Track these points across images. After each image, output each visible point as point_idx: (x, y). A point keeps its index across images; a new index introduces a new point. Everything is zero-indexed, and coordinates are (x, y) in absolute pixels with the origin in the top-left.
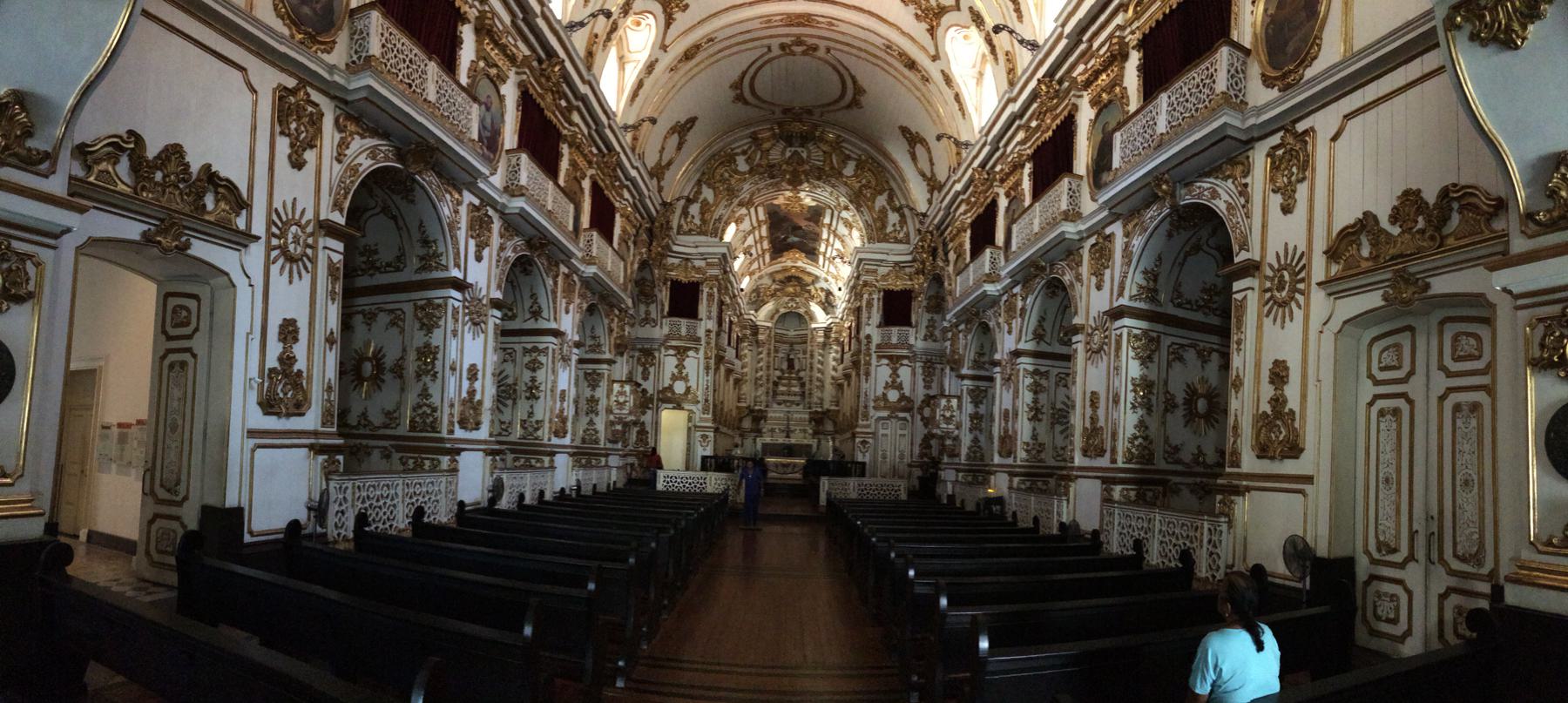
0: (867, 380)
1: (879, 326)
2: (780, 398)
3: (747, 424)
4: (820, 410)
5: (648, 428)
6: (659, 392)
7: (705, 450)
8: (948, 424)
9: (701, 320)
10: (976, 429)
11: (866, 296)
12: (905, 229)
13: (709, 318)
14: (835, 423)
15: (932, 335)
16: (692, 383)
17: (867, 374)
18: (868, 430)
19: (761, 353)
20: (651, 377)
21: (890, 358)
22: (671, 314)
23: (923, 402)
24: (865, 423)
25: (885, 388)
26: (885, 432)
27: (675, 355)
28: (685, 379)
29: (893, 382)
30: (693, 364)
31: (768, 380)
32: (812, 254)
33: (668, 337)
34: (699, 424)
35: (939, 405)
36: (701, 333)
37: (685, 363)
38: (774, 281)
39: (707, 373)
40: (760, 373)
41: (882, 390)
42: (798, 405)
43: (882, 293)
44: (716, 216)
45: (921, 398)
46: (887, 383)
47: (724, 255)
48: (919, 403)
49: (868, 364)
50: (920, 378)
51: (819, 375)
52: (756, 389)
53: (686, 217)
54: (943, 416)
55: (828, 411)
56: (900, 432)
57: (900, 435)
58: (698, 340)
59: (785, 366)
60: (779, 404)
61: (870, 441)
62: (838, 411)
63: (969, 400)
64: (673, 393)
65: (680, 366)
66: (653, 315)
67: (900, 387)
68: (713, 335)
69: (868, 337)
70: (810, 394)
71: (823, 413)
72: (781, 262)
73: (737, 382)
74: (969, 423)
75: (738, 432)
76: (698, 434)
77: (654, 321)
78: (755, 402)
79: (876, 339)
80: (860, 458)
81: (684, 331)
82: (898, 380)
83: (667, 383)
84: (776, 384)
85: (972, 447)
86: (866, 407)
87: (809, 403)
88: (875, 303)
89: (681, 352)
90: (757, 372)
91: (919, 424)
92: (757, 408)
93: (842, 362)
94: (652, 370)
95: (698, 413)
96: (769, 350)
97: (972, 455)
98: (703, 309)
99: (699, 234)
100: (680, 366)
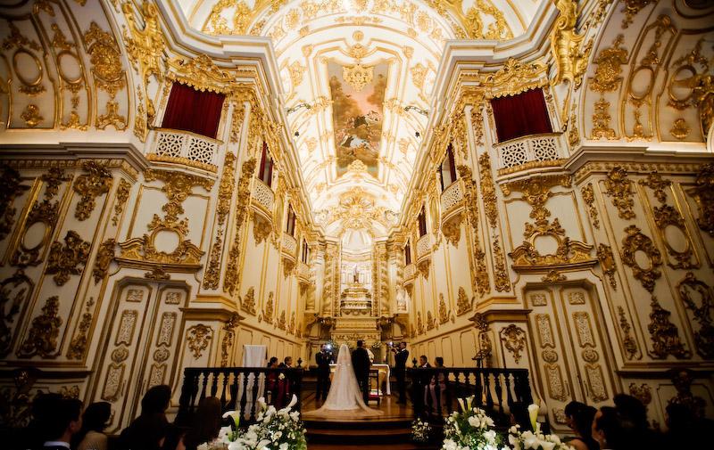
0: (493, 223)
2: (347, 307)
3: (315, 332)
4: (387, 316)
5: (62, 313)
6: (111, 245)
7: (197, 356)
11: (468, 110)
12: (506, 30)
13: (234, 140)
14: (403, 327)
15: (605, 128)
17: (493, 216)
20: (95, 215)
22: (169, 123)
23: (630, 238)
24: (504, 294)
25: (527, 236)
27: (164, 190)
28: (181, 229)
30: (196, 208)
31: (336, 291)
32: (372, 163)
34: (191, 306)
37: (184, 205)
39: (221, 221)
40: (328, 284)
42: (364, 313)
44: (256, 21)
45: (621, 236)
46: (529, 228)
47: (259, 57)
48: (620, 245)
49: (490, 199)
50: (603, 201)
51: (384, 283)
52: (325, 299)
55: (397, 315)
56: (571, 310)
57: (576, 315)
58: (214, 169)
59: (352, 279)
60: (347, 314)
61: (523, 326)
62: (407, 315)
64: (151, 251)
65: (174, 208)
66: (122, 111)
67: (555, 230)
68: (238, 166)
69: (485, 161)
70: (376, 302)
71: (390, 319)
73: (304, 287)
75: (306, 340)
76: (189, 324)
77: (122, 120)
78: (324, 310)
79: (497, 162)
80: (511, 364)
81: (185, 151)
82: (551, 220)
83: (140, 231)
84: (344, 296)
86: (501, 268)
87: (376, 311)
88: (485, 114)
89: (178, 182)
90: (325, 282)
91: (637, 286)
92: (325, 316)
93: (408, 261)
94: (99, 201)
96: (337, 264)
98: (224, 128)
100: (174, 208)
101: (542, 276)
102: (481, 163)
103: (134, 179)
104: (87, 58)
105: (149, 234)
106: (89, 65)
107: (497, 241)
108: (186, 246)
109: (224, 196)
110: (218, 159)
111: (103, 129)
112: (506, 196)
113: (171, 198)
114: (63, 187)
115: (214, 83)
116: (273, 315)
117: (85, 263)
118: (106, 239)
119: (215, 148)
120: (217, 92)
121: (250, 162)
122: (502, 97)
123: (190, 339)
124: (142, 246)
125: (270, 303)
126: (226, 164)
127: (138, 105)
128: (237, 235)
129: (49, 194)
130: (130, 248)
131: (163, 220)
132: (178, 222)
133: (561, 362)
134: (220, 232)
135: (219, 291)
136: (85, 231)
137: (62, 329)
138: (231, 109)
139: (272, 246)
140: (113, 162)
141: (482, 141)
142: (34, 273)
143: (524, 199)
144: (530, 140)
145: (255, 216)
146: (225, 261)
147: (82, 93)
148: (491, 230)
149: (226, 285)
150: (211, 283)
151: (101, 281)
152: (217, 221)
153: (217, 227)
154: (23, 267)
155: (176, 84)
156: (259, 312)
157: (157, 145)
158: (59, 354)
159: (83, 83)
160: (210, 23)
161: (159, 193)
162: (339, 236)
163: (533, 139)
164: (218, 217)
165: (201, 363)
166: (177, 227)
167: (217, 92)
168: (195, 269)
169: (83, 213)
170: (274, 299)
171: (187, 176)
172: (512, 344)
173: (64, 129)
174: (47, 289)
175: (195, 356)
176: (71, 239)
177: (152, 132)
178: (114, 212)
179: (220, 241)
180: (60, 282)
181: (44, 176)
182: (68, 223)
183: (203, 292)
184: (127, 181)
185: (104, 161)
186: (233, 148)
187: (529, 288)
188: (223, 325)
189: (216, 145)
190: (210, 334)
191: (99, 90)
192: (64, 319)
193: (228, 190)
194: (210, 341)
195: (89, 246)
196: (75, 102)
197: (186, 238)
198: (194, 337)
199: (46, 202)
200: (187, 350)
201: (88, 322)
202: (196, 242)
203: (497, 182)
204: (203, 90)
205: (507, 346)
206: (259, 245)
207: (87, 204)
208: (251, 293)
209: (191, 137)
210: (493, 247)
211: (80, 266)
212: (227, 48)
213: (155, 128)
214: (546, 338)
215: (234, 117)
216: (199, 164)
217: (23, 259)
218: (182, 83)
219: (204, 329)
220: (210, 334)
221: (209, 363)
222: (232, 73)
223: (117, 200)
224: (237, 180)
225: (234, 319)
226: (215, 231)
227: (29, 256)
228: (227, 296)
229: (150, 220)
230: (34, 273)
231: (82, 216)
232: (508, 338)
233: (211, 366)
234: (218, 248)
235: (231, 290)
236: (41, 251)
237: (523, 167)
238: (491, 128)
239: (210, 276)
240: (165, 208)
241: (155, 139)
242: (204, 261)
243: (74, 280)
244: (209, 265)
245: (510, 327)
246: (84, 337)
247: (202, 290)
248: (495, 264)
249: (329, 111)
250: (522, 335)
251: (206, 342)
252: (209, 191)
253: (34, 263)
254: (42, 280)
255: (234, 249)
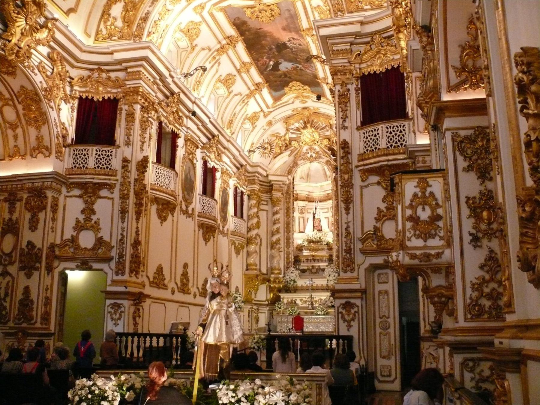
1: (358, 129)
5: (34, 296)
6: (52, 246)
7: (116, 325)
8: (426, 236)
9: (119, 146)
10: (490, 234)
16: (105, 234)
18: (356, 286)
19: (276, 213)
20: (41, 226)
21: (378, 171)
25: (377, 220)
26: (383, 287)
27: (80, 197)
28: (96, 227)
29: (387, 209)
33: (70, 172)
34: (109, 289)
35: (402, 194)
36: (116, 164)
37: (96, 207)
38: (287, 130)
39: (123, 219)
41: (374, 222)
43: (359, 81)
44: (141, 14)
53: (105, 22)
54: (414, 219)
58: (114, 173)
61: (358, 302)
63: (462, 163)
64: (77, 247)
65: (89, 211)
72: (286, 104)
74: (468, 225)
76: (108, 302)
77: (47, 149)
80: (344, 332)
81: (91, 162)
85: (483, 281)
90: (273, 234)
94: (41, 215)
95: (110, 273)
97: (487, 303)
99: (121, 38)
100: (89, 211)
101: (383, 258)
102: (343, 148)
103: (59, 192)
104: (20, 107)
105: (75, 234)
106: (21, 112)
107: (348, 227)
108: (100, 241)
109: (124, 197)
110: (116, 164)
111: (36, 157)
112: (363, 181)
113: (86, 202)
114: (18, 204)
115: (109, 90)
116: (191, 284)
117: (40, 263)
118: (49, 244)
119: (113, 154)
120: (112, 98)
121: (142, 161)
122: (369, 73)
123: (110, 312)
124: (71, 244)
125: (185, 275)
126: (123, 167)
127: (56, 133)
128: (137, 228)
129: (11, 212)
130: (64, 247)
131: (82, 222)
132: (93, 222)
133: (391, 330)
134: (123, 229)
135: (126, 277)
136: (36, 238)
137: (35, 306)
138: (124, 113)
139: (182, 217)
140: (46, 184)
141: (346, 124)
142: (13, 269)
143: (379, 183)
144: (384, 126)
145: (156, 200)
146: (129, 252)
147: (19, 131)
148: (344, 216)
149: (131, 271)
150: (120, 270)
151: (51, 273)
152: (120, 220)
153: (120, 224)
154: (5, 266)
155: (81, 99)
156: (171, 285)
157: (71, 161)
158: (36, 322)
159: (19, 124)
160: (102, 23)
161: (77, 199)
162: (290, 172)
163: (386, 125)
164: (120, 215)
165: (119, 329)
166: (92, 226)
167: (112, 98)
168: (108, 260)
169: (33, 226)
170: (190, 271)
171: (95, 184)
172: (346, 317)
173: (11, 160)
174: (22, 281)
175: (115, 324)
176: (30, 246)
177: (67, 149)
178: (51, 223)
179: (123, 237)
180: (29, 276)
181: (5, 198)
182: (27, 235)
183: (115, 278)
184: (55, 196)
185: (40, 184)
186: (127, 152)
187: (374, 268)
188: (132, 302)
189: (114, 150)
190: (122, 309)
191: (30, 128)
192: (35, 299)
193: (126, 192)
194: (123, 314)
195: (41, 250)
196: (16, 137)
197: (100, 235)
198: (113, 311)
199: (10, 219)
200: (109, 320)
201: (48, 301)
202: (106, 238)
203: (357, 167)
204: (101, 100)
205: (342, 317)
206: (165, 224)
207: (35, 220)
208: (160, 270)
209: (95, 148)
210: (344, 232)
211: (38, 265)
212: (118, 56)
213: (69, 146)
214: (384, 311)
215: (127, 120)
216: (103, 172)
217: (5, 260)
218: (84, 97)
219: (119, 306)
220: (122, 309)
221: (124, 330)
222: (121, 75)
223: (52, 214)
224: (132, 182)
225: (140, 297)
226: (120, 228)
227: (7, 258)
228: (134, 279)
229: (73, 223)
230: (13, 269)
231: (33, 228)
232: (344, 312)
233: (126, 332)
234: (123, 243)
235: (137, 273)
236: (13, 254)
237: (375, 155)
238: (357, 108)
239: (119, 265)
240: (83, 212)
241: (70, 154)
242: (114, 253)
243: (36, 274)
244: (117, 257)
245: (346, 303)
246: (47, 312)
247: (114, 275)
248: (344, 248)
249: (241, 47)
250: (356, 309)
251: (120, 315)
252: (112, 193)
253: (11, 263)
254: (18, 274)
255: (135, 241)
